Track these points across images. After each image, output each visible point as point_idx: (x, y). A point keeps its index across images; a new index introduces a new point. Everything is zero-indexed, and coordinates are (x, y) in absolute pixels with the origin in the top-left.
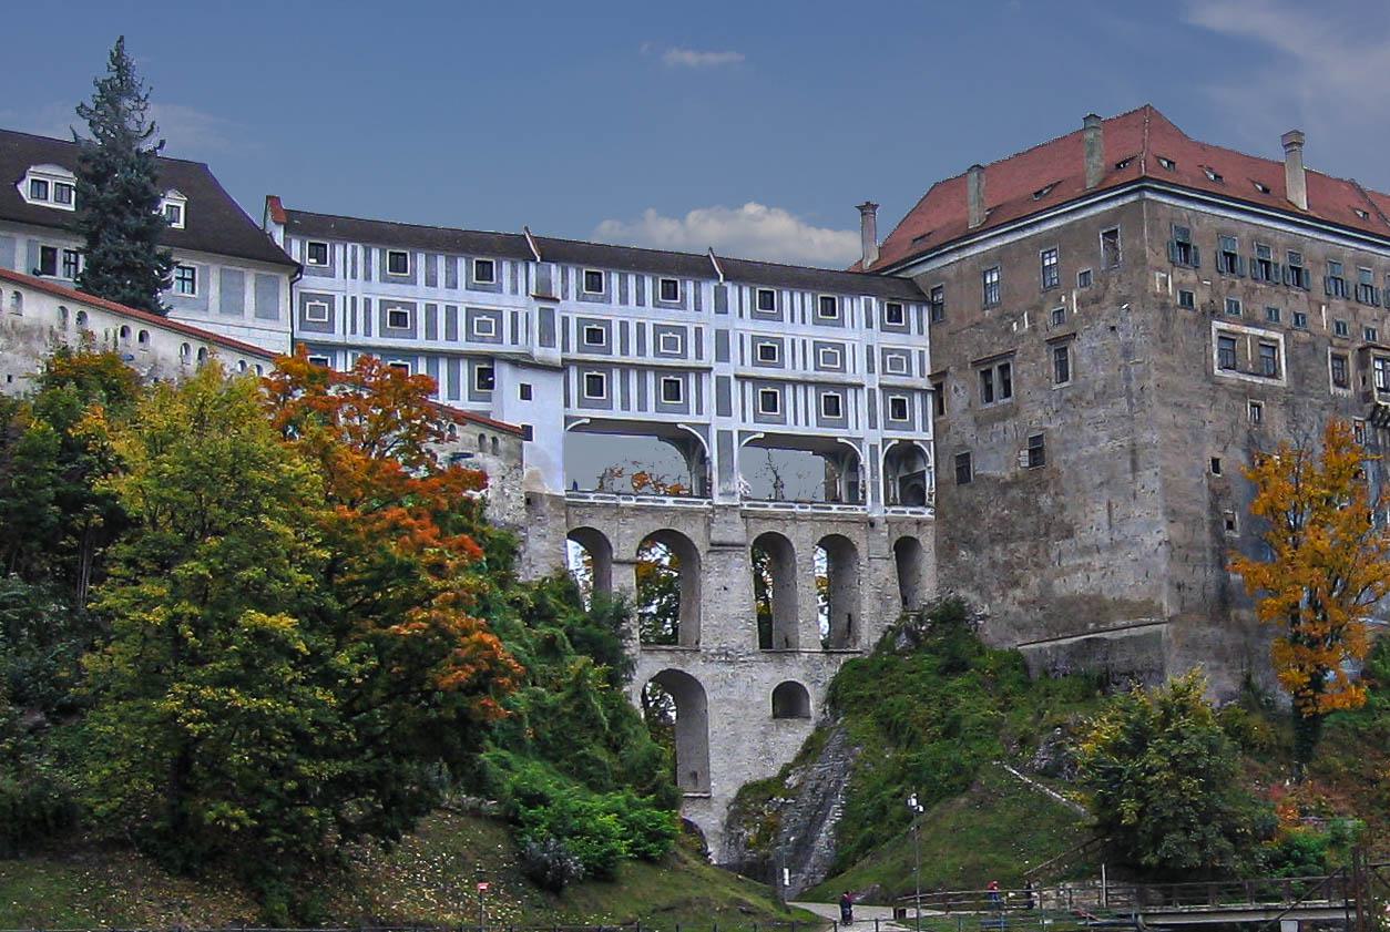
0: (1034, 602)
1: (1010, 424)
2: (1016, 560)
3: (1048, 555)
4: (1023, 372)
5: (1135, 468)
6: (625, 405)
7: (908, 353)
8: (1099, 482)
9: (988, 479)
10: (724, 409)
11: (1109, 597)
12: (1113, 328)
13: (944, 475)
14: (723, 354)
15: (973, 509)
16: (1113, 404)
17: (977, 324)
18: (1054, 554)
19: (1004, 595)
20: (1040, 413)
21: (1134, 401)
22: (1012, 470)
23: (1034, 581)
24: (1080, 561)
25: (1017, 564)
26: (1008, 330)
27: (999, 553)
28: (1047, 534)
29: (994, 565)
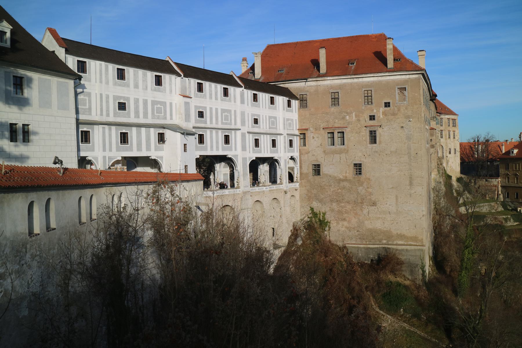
0: (354, 228)
1: (343, 156)
2: (345, 210)
3: (361, 210)
4: (351, 136)
5: (411, 184)
6: (212, 149)
7: (292, 120)
8: (391, 186)
9: (330, 176)
10: (244, 148)
11: (394, 232)
12: (402, 127)
13: (305, 171)
14: (243, 123)
15: (321, 186)
16: (401, 157)
17: (327, 113)
18: (365, 211)
19: (338, 223)
20: (360, 154)
21: (412, 158)
22: (344, 175)
23: (354, 221)
24: (381, 216)
25: (345, 212)
26: (344, 118)
27: (335, 205)
28: (362, 203)
29: (332, 210)
